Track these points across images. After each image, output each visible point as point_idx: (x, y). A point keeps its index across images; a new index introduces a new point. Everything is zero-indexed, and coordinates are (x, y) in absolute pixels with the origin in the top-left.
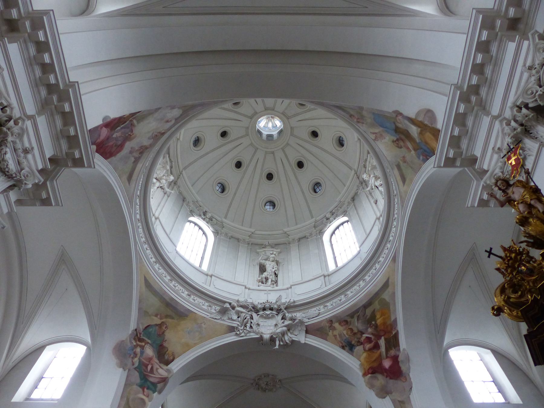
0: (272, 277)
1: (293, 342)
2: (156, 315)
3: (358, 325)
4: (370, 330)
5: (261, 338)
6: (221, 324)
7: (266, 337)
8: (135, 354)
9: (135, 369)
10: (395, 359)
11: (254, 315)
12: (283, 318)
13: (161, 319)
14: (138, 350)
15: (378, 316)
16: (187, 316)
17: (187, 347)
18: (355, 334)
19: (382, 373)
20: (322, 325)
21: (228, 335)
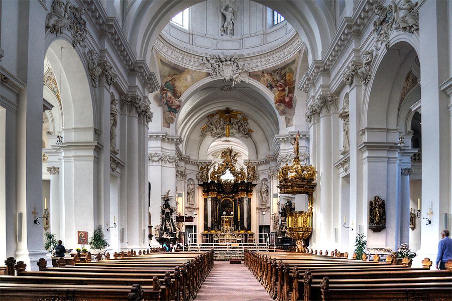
0: (230, 27)
1: (242, 81)
2: (169, 76)
3: (277, 77)
4: (282, 81)
5: (225, 79)
6: (202, 72)
7: (227, 78)
8: (164, 98)
9: (165, 104)
10: (291, 98)
11: (220, 64)
12: (237, 66)
13: (171, 77)
14: (164, 95)
15: (287, 76)
16: (184, 71)
17: (187, 87)
18: (275, 81)
19: (284, 103)
20: (258, 73)
21: (206, 78)
